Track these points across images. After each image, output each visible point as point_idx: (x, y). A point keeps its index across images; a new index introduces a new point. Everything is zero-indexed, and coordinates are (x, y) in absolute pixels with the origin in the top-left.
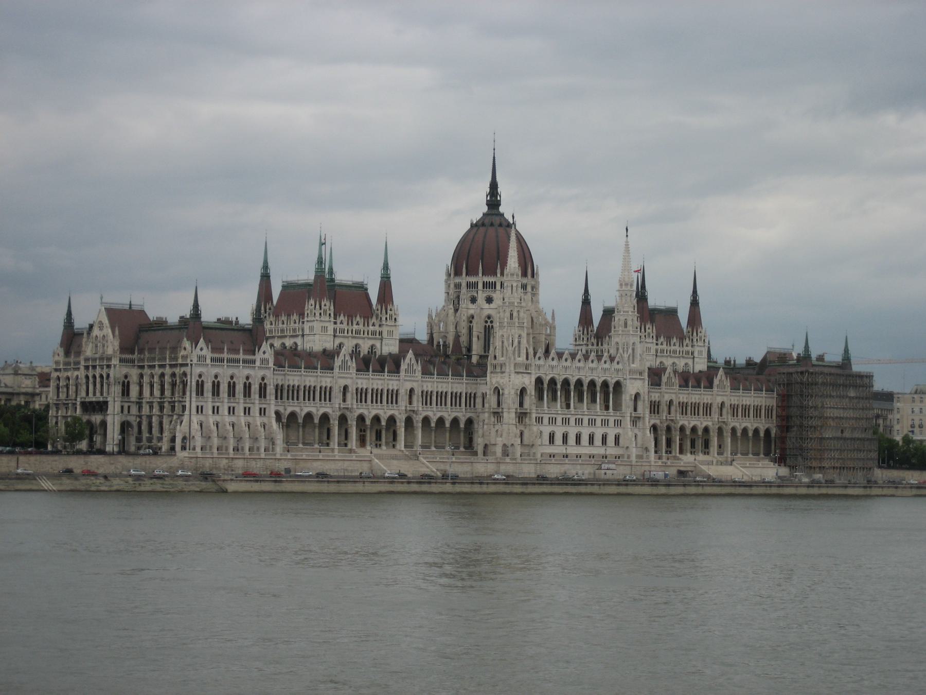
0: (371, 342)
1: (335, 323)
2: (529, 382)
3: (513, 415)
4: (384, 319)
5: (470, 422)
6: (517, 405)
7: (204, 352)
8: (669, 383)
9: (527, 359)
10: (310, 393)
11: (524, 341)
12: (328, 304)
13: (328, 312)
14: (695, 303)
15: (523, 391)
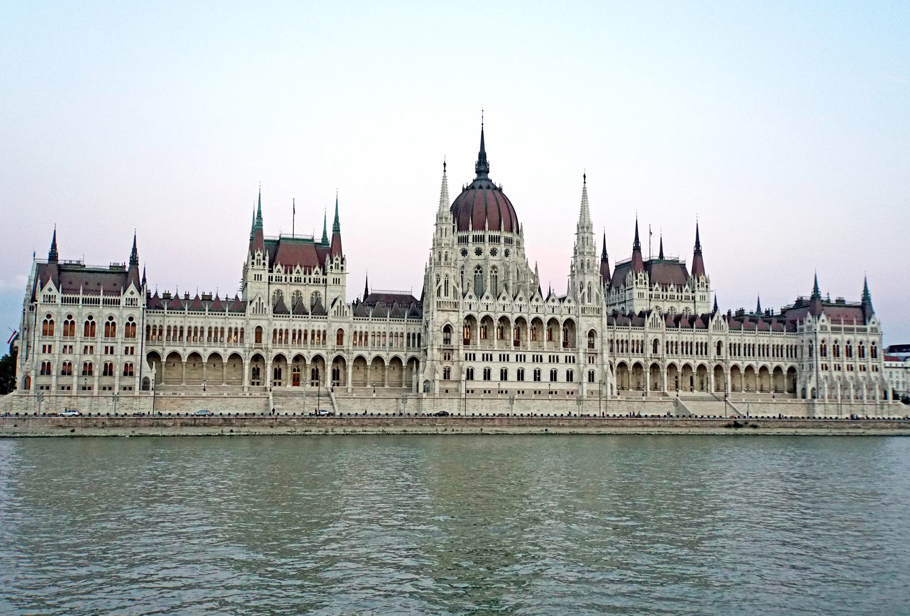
0: (313, 289)
1: (271, 271)
2: (456, 320)
3: (435, 351)
4: (329, 267)
5: (413, 360)
6: (441, 342)
7: (51, 294)
8: (654, 325)
9: (455, 296)
10: (215, 334)
11: (452, 283)
12: (262, 254)
13: (262, 262)
14: (698, 252)
15: (448, 329)
